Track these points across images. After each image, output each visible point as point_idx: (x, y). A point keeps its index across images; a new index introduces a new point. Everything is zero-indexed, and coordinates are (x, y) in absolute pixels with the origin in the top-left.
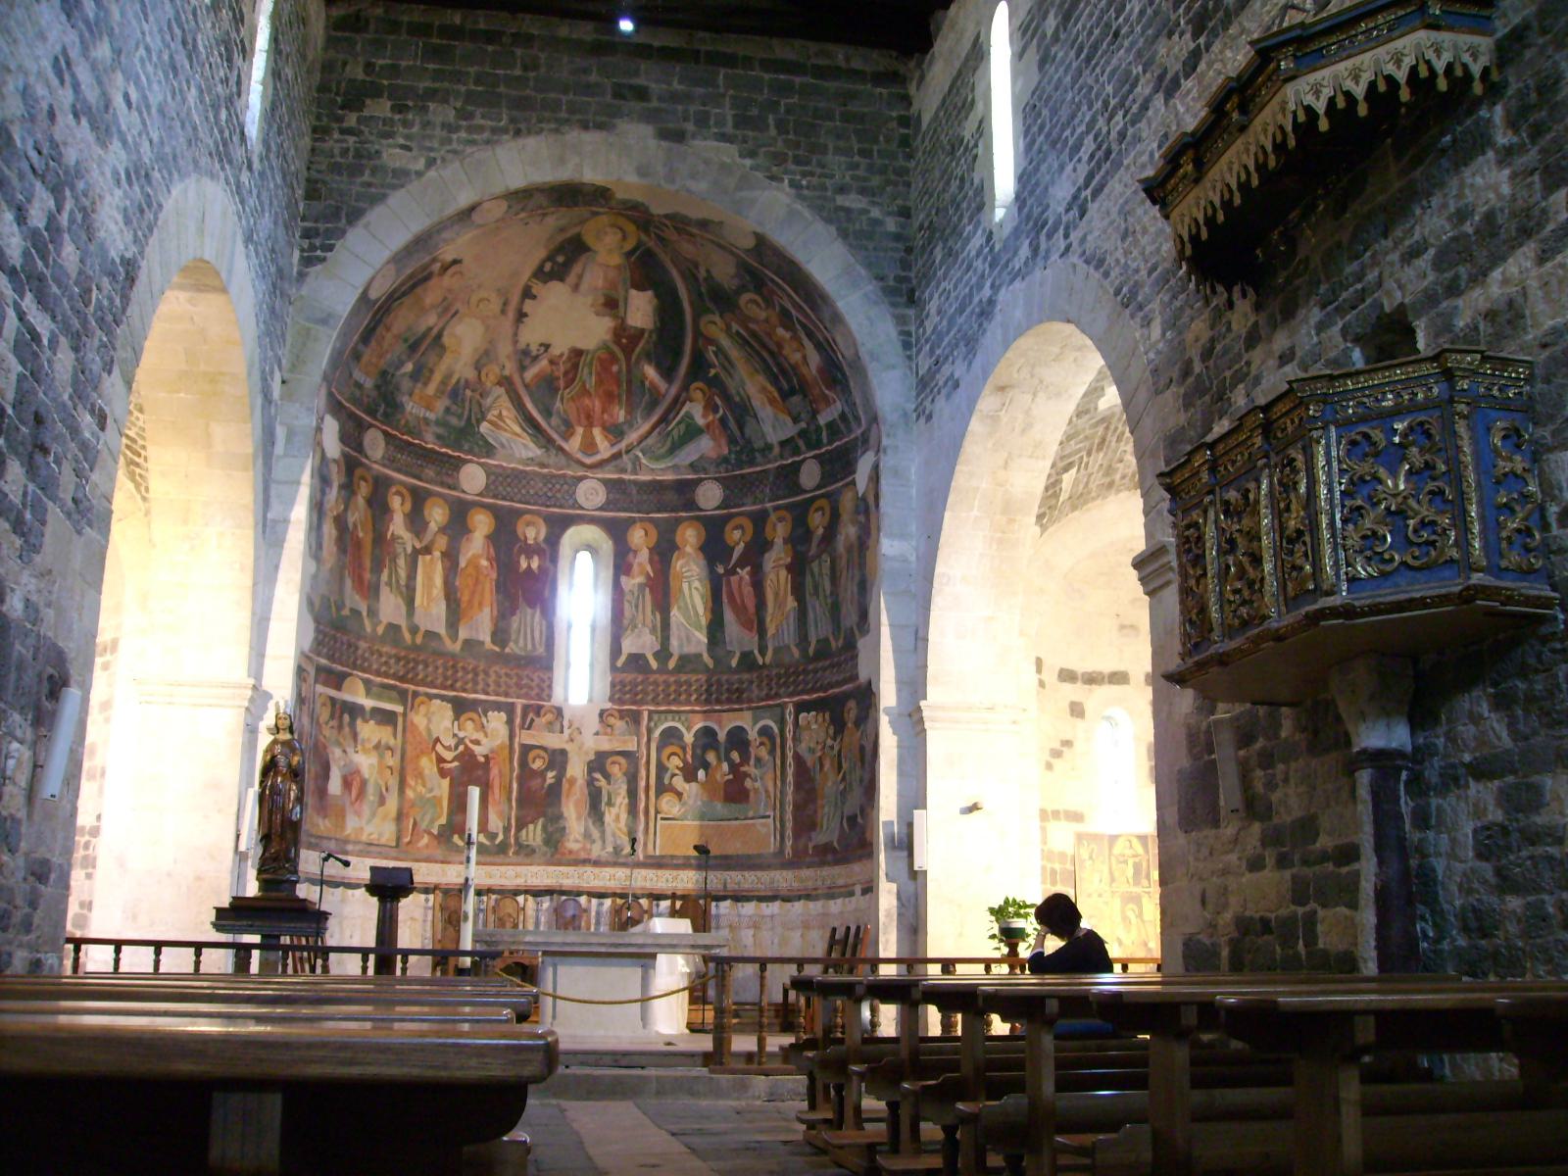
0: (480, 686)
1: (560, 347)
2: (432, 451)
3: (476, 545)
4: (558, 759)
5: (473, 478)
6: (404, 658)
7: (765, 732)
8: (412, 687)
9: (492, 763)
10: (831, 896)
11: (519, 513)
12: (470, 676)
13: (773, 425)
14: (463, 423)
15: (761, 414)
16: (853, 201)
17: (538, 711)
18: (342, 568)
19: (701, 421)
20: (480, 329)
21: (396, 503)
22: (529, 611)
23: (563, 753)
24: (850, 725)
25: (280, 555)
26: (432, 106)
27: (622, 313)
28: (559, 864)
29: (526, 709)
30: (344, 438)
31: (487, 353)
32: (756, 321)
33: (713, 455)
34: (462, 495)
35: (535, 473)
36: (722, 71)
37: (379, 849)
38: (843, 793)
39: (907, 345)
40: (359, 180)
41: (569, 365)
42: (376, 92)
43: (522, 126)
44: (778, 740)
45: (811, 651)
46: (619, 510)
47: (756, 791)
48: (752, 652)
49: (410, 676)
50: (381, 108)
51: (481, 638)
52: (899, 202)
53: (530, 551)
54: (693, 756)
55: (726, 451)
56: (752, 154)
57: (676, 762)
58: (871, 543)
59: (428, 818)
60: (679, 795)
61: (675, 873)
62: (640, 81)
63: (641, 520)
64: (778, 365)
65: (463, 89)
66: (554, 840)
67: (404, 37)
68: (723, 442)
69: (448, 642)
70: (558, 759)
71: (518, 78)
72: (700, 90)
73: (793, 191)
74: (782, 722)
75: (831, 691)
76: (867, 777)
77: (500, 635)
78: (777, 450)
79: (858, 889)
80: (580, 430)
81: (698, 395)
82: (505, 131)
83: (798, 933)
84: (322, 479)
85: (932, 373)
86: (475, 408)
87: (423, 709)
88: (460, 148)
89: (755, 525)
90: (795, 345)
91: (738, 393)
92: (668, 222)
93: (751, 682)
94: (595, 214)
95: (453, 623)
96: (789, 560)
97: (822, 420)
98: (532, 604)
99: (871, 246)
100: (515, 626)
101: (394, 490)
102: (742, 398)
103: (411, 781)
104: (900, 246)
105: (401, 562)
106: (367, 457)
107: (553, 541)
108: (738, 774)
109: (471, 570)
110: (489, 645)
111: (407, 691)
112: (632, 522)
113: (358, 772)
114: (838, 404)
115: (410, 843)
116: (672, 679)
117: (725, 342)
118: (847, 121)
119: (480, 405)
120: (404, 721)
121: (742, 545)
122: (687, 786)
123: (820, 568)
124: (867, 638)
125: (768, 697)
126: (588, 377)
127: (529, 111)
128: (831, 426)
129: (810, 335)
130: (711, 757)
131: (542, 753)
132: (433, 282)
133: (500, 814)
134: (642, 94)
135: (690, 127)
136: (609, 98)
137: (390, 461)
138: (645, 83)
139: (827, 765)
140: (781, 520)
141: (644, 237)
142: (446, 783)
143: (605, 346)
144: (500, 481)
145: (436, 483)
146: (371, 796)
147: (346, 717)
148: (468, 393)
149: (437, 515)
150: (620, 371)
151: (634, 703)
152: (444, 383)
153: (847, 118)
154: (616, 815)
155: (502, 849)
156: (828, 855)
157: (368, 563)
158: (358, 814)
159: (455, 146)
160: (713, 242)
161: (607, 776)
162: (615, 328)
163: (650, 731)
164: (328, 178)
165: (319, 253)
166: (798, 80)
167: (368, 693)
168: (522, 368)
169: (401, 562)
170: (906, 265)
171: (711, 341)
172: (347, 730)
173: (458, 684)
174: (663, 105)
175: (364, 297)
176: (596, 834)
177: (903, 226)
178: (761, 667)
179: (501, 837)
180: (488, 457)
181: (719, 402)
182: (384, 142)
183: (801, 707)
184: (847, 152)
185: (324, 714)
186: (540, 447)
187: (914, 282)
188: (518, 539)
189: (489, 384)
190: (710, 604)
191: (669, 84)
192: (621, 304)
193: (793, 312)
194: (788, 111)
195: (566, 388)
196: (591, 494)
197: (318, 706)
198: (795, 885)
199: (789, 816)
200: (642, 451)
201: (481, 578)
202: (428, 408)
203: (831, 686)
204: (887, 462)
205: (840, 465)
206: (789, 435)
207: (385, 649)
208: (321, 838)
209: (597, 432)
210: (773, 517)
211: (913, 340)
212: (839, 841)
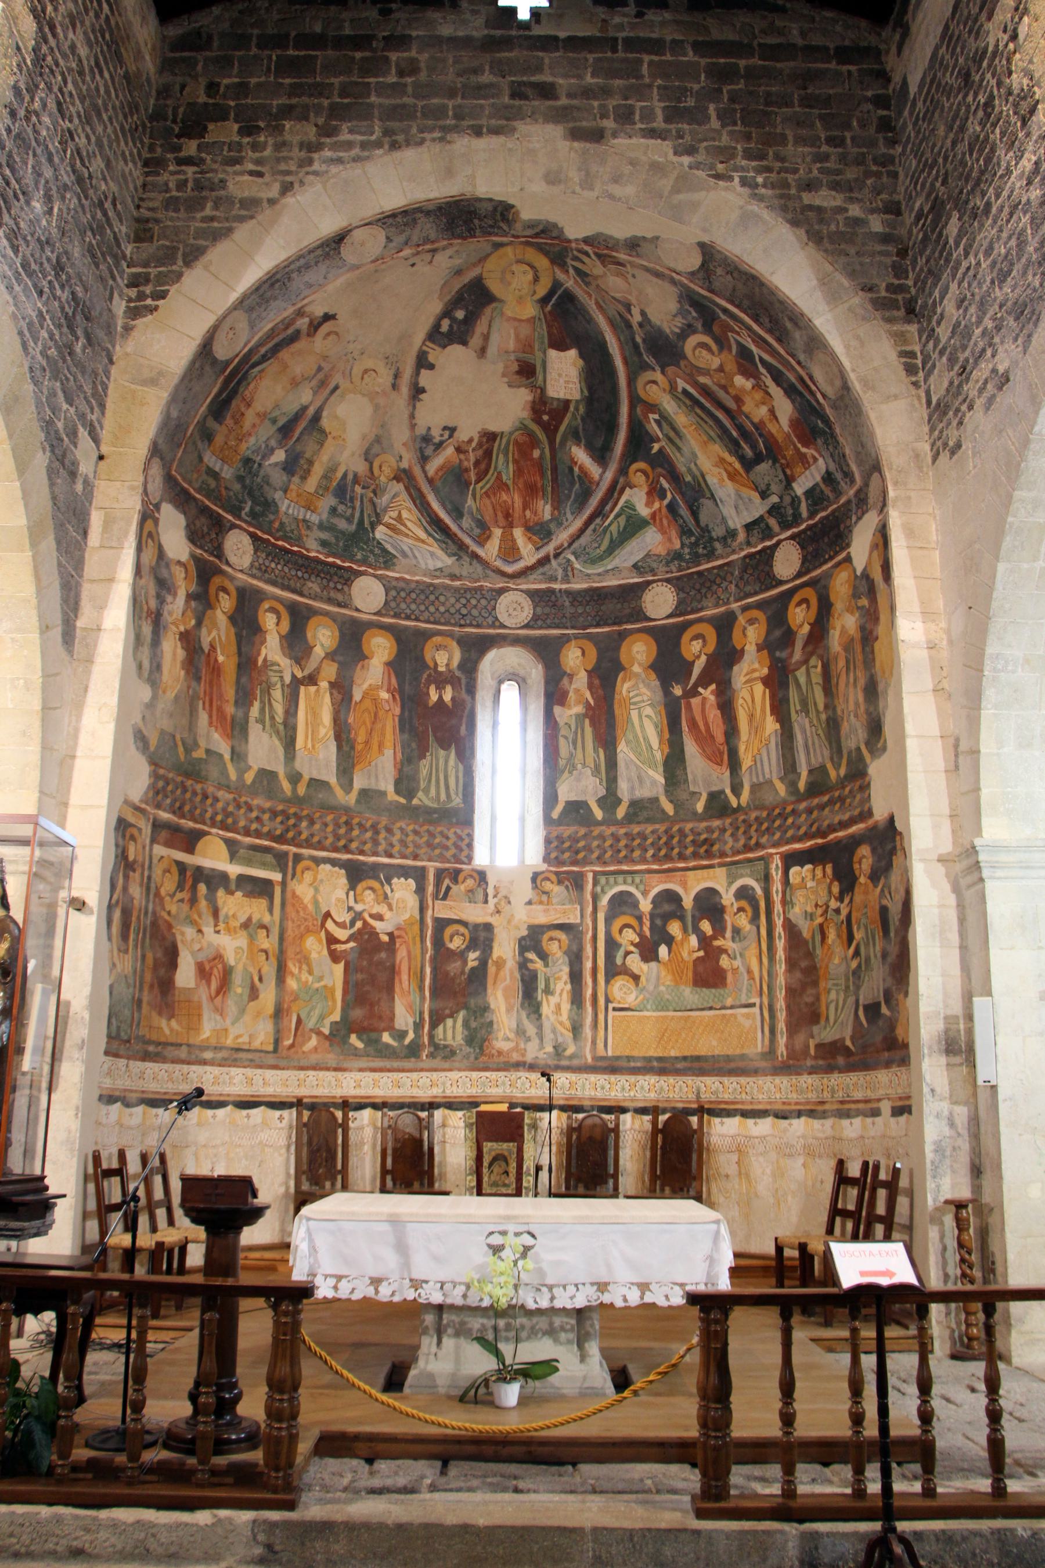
0: (381, 848)
1: (468, 431)
2: (317, 560)
3: (374, 673)
4: (481, 936)
5: (368, 594)
6: (283, 812)
7: (743, 893)
8: (294, 849)
9: (398, 941)
10: (847, 1115)
12: (369, 834)
13: (735, 504)
14: (354, 527)
17: (455, 876)
18: (193, 701)
19: (644, 511)
20: (369, 410)
21: (269, 621)
22: (442, 753)
23: (488, 927)
24: (862, 880)
25: (88, 672)
26: (288, 125)
27: (540, 382)
28: (486, 1069)
29: (439, 875)
30: (193, 536)
31: (378, 440)
32: (706, 372)
33: (661, 550)
35: (447, 587)
36: (646, 58)
37: (250, 1056)
38: (856, 973)
39: (910, 370)
40: (199, 215)
41: (480, 452)
42: (221, 115)
43: (400, 138)
44: (762, 904)
45: (802, 785)
46: (549, 627)
47: (735, 971)
48: (723, 792)
49: (290, 835)
50: (227, 131)
51: (382, 786)
52: (884, 196)
53: (441, 681)
54: (651, 929)
55: (677, 545)
56: (691, 151)
57: (630, 936)
58: (881, 630)
59: (317, 1012)
60: (636, 978)
61: (632, 1078)
62: (546, 77)
63: (576, 637)
64: (740, 428)
65: (326, 103)
66: (478, 1038)
67: (254, 51)
68: (674, 534)
69: (339, 792)
70: (481, 936)
71: (393, 86)
72: (618, 82)
73: (746, 191)
74: (766, 879)
75: (831, 837)
76: (894, 950)
77: (406, 784)
78: (742, 536)
79: (886, 1107)
80: (497, 532)
81: (640, 479)
82: (378, 144)
83: (800, 1160)
85: (955, 390)
86: (368, 510)
87: (308, 876)
88: (324, 167)
89: (719, 636)
90: (758, 395)
91: (689, 470)
93: (723, 830)
97: (800, 488)
98: (444, 744)
99: (852, 251)
100: (424, 772)
101: (266, 605)
102: (694, 477)
103: (292, 967)
104: (891, 248)
105: (277, 694)
106: (228, 564)
107: (469, 667)
108: (710, 951)
109: (368, 703)
110: (392, 796)
111: (286, 854)
113: (219, 957)
114: (821, 461)
115: (292, 1046)
116: (622, 831)
117: (669, 405)
118: (811, 107)
119: (374, 505)
120: (283, 892)
121: (704, 658)
122: (645, 967)
123: (807, 677)
124: (885, 757)
125: (747, 848)
126: (504, 467)
129: (778, 378)
130: (674, 928)
131: (462, 929)
133: (410, 1008)
134: (547, 91)
135: (609, 124)
136: (506, 100)
137: (260, 571)
138: (550, 79)
139: (832, 935)
140: (751, 621)
141: (561, 276)
142: (339, 969)
143: (523, 427)
146: (238, 987)
147: (202, 888)
148: (358, 489)
149: (323, 637)
151: (574, 863)
153: (808, 102)
156: (833, 1057)
157: (230, 693)
158: (221, 1011)
159: (316, 166)
160: (647, 270)
161: (543, 956)
163: (595, 898)
164: (159, 215)
165: (149, 302)
166: (742, 63)
167: (233, 856)
168: (424, 459)
169: (277, 694)
170: (899, 271)
171: (653, 408)
172: (203, 904)
173: (354, 846)
174: (575, 102)
176: (531, 1030)
177: (892, 225)
178: (736, 811)
179: (411, 1035)
180: (387, 568)
181: (666, 485)
182: (229, 169)
183: (791, 860)
184: (814, 141)
185: (169, 885)
187: (913, 291)
188: (425, 666)
189: (383, 479)
190: (667, 735)
191: (580, 77)
194: (732, 100)
195: (477, 482)
196: (514, 609)
197: (157, 872)
198: (794, 1097)
199: (781, 1004)
201: (381, 713)
202: (308, 508)
203: (832, 829)
204: (895, 519)
205: (826, 539)
207: (255, 802)
208: (166, 1044)
209: (518, 533)
210: (741, 620)
211: (919, 362)
212: (852, 1038)
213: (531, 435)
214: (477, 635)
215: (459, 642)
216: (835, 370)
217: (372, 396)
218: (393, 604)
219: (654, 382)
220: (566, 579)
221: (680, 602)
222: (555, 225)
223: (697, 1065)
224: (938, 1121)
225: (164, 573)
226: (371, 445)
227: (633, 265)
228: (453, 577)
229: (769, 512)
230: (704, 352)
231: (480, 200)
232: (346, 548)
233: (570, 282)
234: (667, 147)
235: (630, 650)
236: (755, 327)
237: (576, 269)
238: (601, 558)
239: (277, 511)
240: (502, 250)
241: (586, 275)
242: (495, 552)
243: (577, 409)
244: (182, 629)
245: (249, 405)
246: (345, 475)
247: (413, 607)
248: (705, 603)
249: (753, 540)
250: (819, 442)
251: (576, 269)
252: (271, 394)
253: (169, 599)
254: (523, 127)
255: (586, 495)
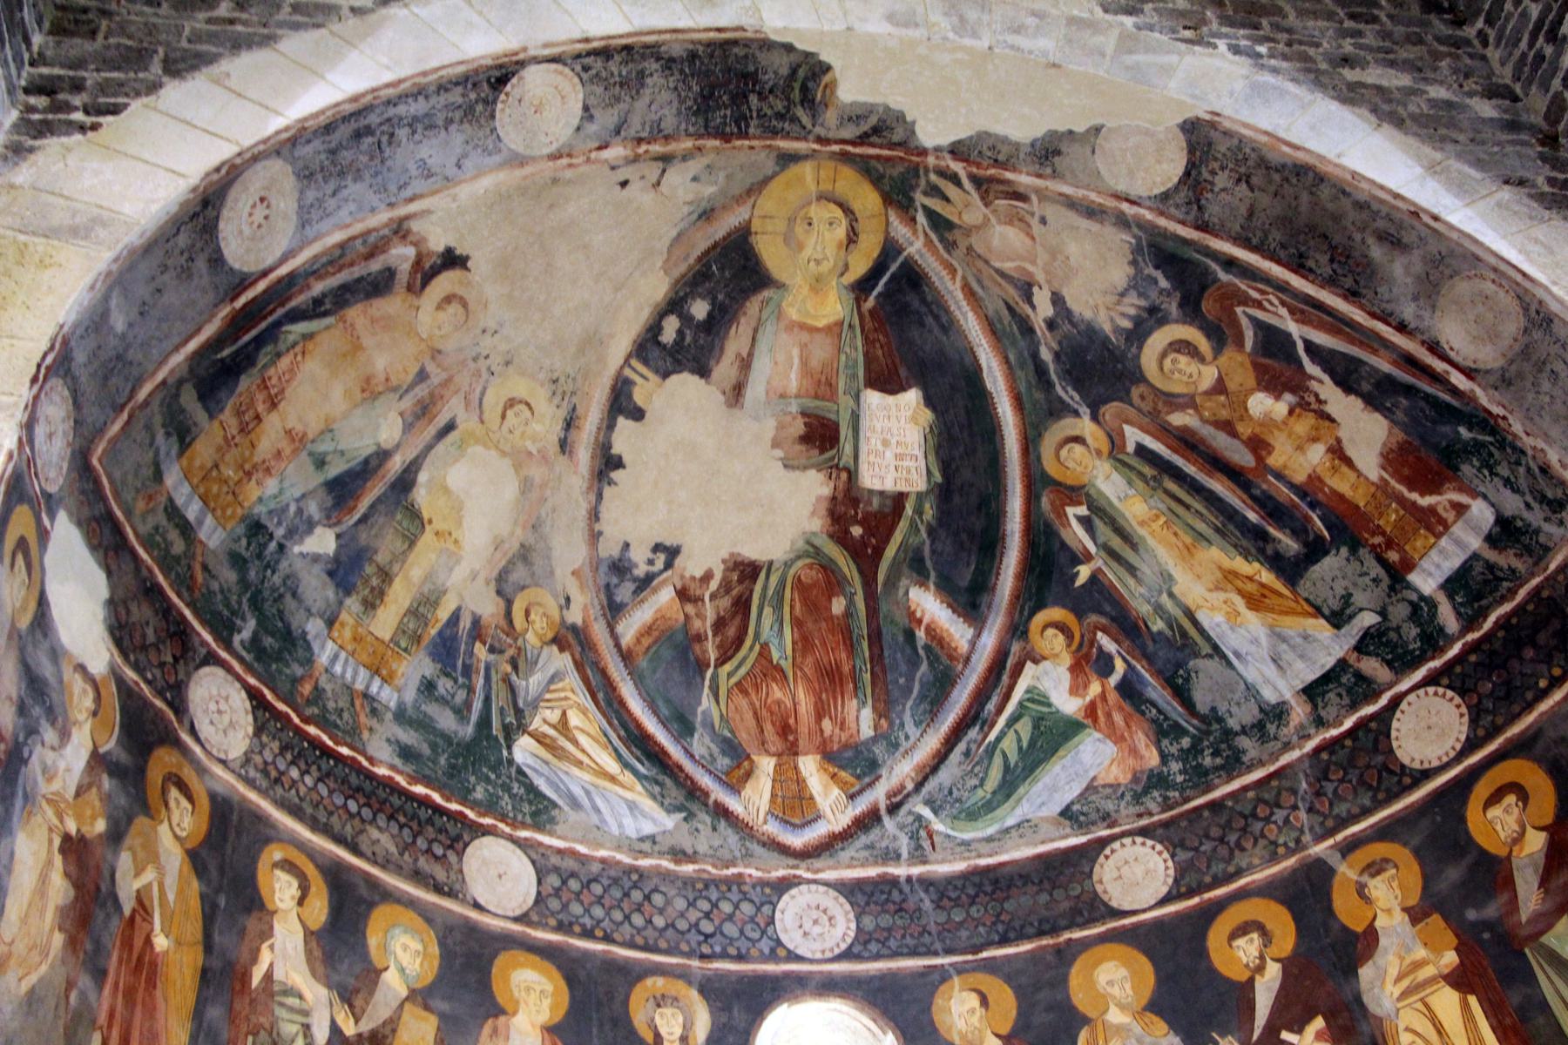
1: (704, 557)
5: (498, 876)
11: (631, 975)
13: (1269, 653)
14: (469, 731)
15: (1231, 641)
16: (1374, 75)
19: (1068, 705)
20: (510, 490)
21: (281, 890)
30: (121, 632)
31: (524, 554)
32: (1188, 402)
33: (1119, 774)
34: (474, 915)
41: (725, 603)
46: (895, 955)
55: (1152, 759)
63: (960, 970)
68: (1141, 739)
78: (1300, 712)
81: (1054, 642)
86: (500, 699)
89: (1297, 919)
90: (1303, 425)
91: (1159, 609)
92: (957, 167)
94: (786, 159)
96: (1450, 958)
97: (1426, 581)
101: (276, 853)
102: (1170, 622)
112: (934, 980)
117: (1109, 484)
119: (512, 690)
121: (1273, 970)
126: (774, 633)
128: (1471, 586)
129: (1346, 375)
132: (391, 305)
141: (900, 230)
143: (813, 551)
144: (562, 882)
145: (399, 870)
148: (480, 651)
149: (404, 954)
150: (849, 613)
152: (419, 610)
160: (1071, 204)
162: (834, 498)
168: (614, 610)
171: (1073, 493)
175: (204, 209)
180: (538, 827)
186: (670, 810)
189: (530, 636)
192: (845, 431)
193: (1293, 328)
195: (721, 662)
196: (814, 922)
200: (928, 802)
206: (1329, 662)
209: (809, 765)
210: (1347, 871)
213: (828, 568)
214: (742, 978)
215: (703, 991)
216: (1506, 301)
217: (520, 458)
218: (554, 904)
219: (1078, 440)
220: (919, 856)
221: (1181, 872)
222: (900, 117)
225: (46, 670)
226: (511, 562)
227: (1043, 196)
228: (679, 855)
229: (1360, 648)
230: (1183, 360)
231: (767, 45)
232: (453, 771)
233: (916, 244)
235: (1091, 983)
236: (1296, 281)
237: (931, 214)
238: (989, 806)
239: (309, 661)
240: (794, 170)
241: (950, 225)
242: (764, 802)
243: (919, 511)
244: (72, 827)
245: (273, 405)
246: (455, 618)
247: (598, 912)
248: (1241, 860)
249: (1329, 713)
250: (1467, 470)
251: (931, 214)
252: (323, 398)
253: (50, 735)
255: (943, 683)
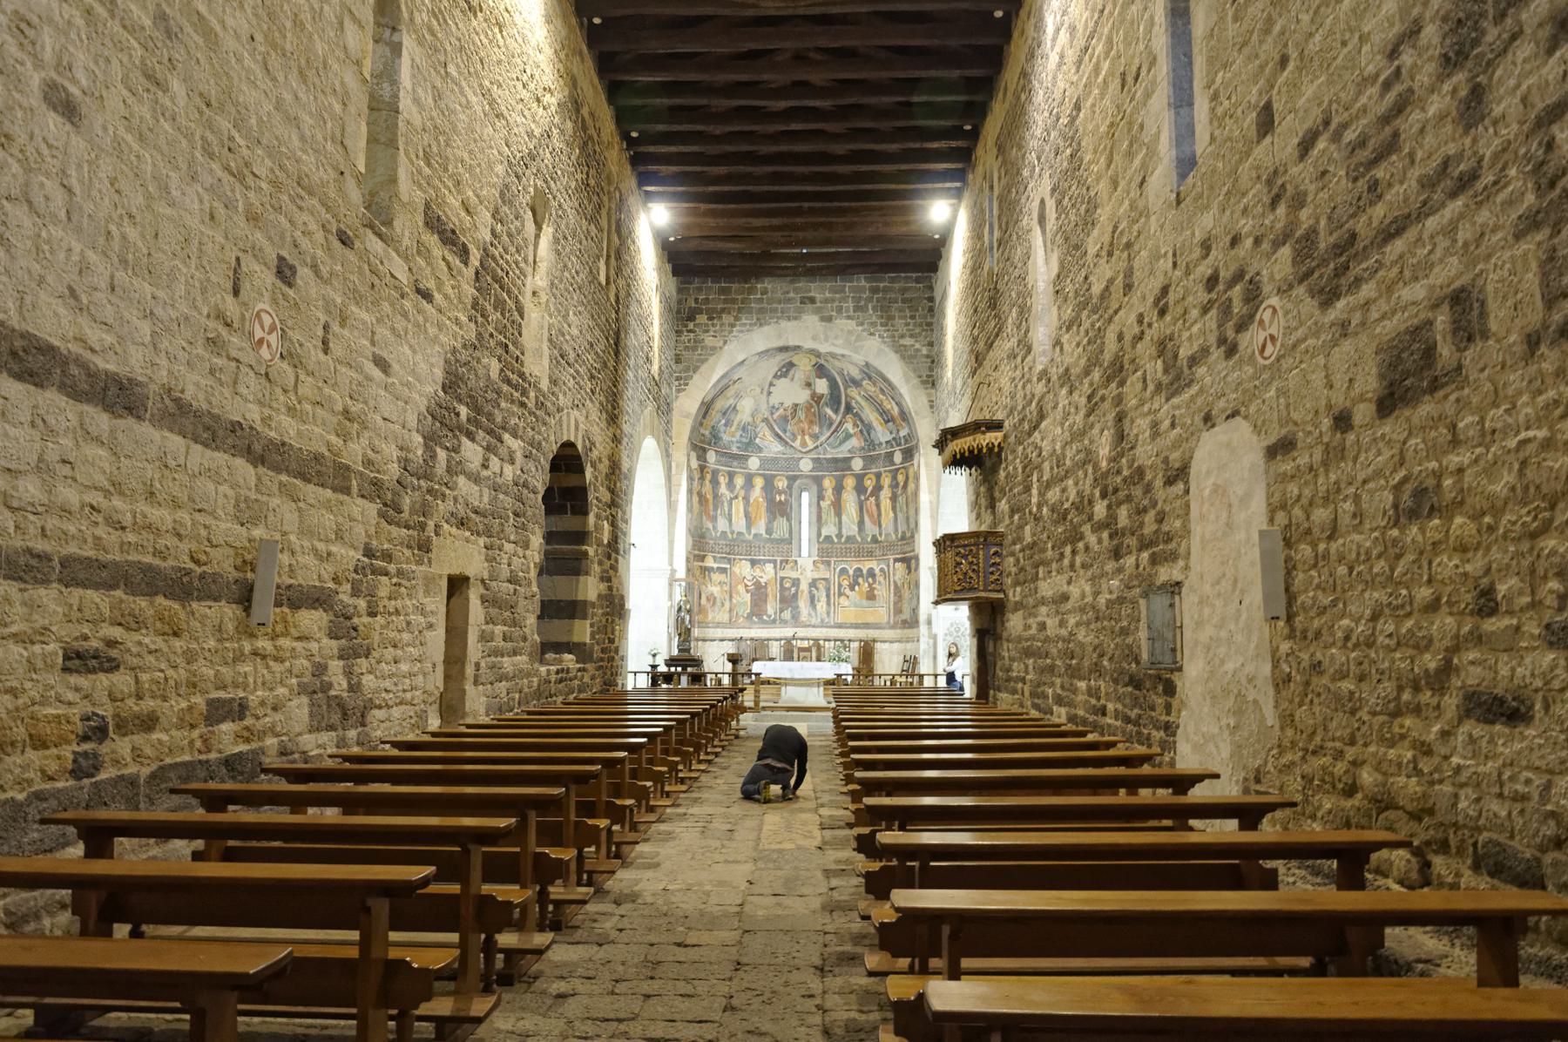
1: (788, 403)
3: (757, 492)
4: (796, 582)
5: (754, 463)
7: (882, 570)
11: (774, 476)
13: (882, 434)
50: (702, 319)
53: (780, 493)
70: (796, 582)
77: (769, 531)
84: (690, 479)
95: (749, 527)
112: (823, 477)
126: (801, 415)
127: (763, 316)
134: (812, 300)
137: (718, 462)
144: (763, 461)
146: (718, 603)
149: (739, 481)
153: (904, 301)
154: (821, 605)
155: (774, 621)
170: (931, 369)
183: (896, 560)
196: (806, 465)
205: (909, 454)
223: (867, 626)
224: (924, 644)
234: (853, 323)
254: (805, 317)
255: (831, 425)
